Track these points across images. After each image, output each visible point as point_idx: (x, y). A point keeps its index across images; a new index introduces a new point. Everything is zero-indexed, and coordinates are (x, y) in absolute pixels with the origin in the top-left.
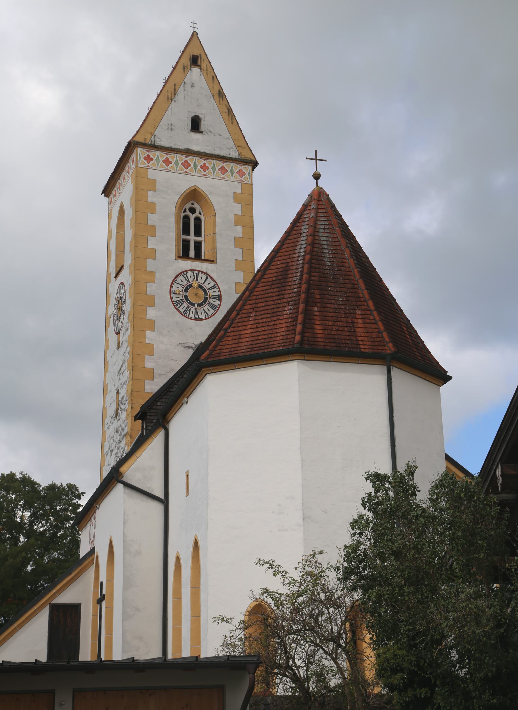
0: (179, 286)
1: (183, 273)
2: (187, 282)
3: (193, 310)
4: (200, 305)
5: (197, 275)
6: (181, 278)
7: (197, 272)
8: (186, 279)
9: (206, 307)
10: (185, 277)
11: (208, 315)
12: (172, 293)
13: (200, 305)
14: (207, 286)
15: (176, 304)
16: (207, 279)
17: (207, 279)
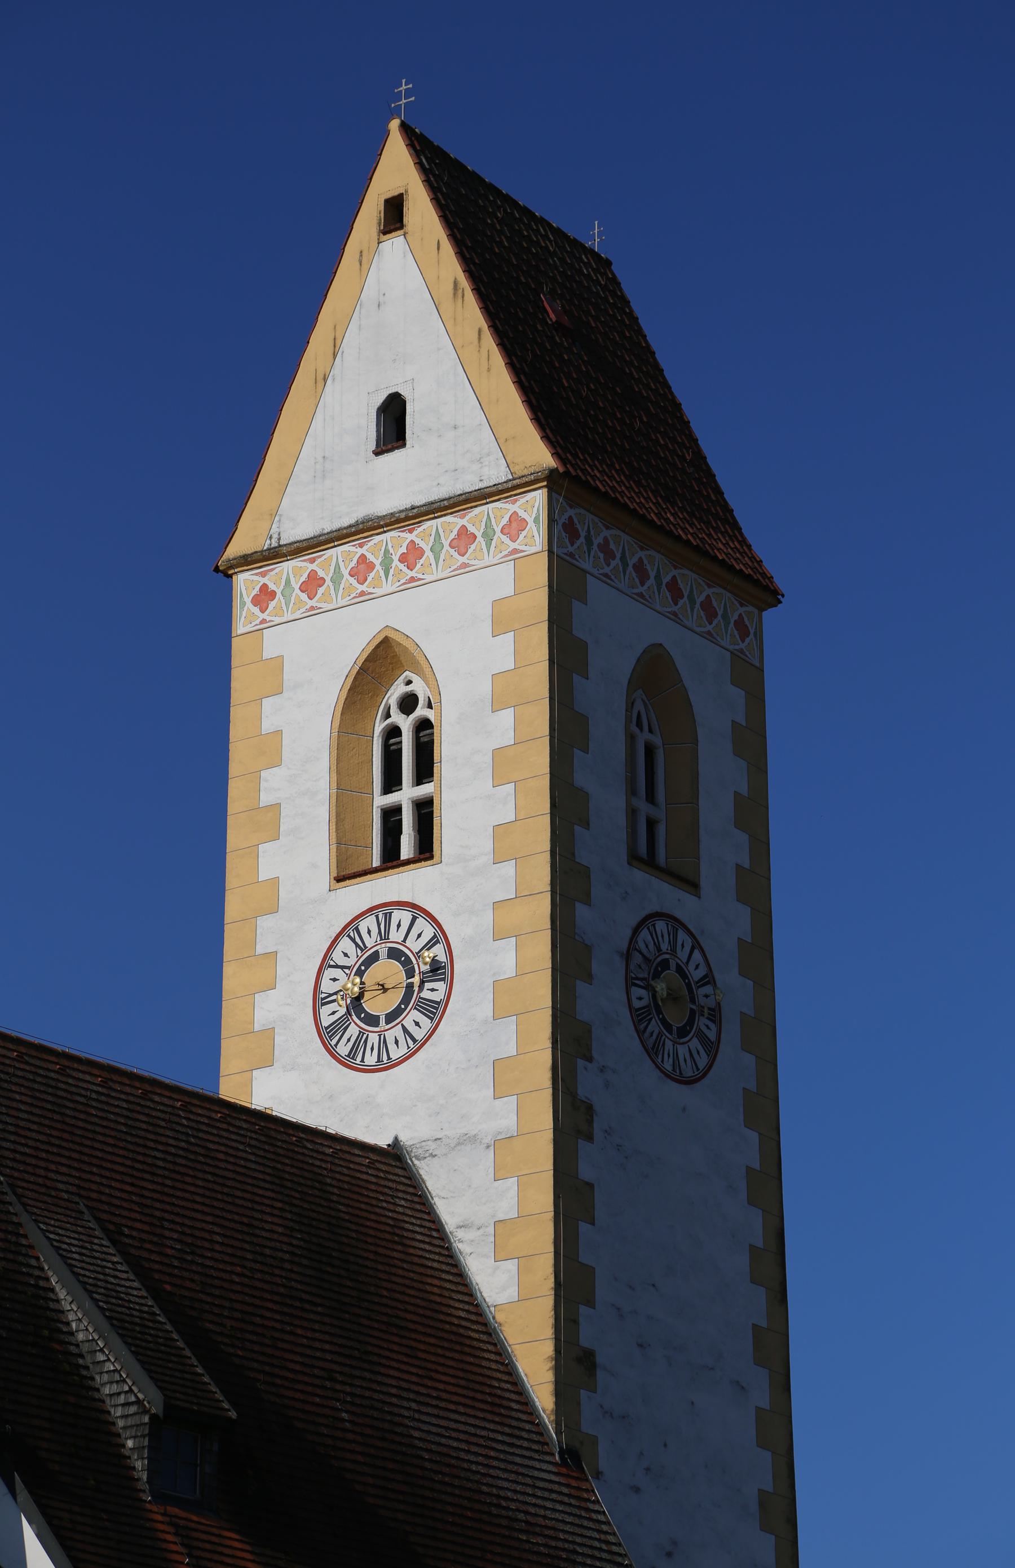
0: (337, 973)
1: (350, 929)
2: (359, 951)
3: (373, 1039)
4: (391, 1017)
5: (388, 917)
6: (346, 944)
7: (384, 910)
8: (357, 945)
9: (412, 1017)
10: (353, 940)
11: (414, 1040)
12: (319, 1000)
13: (391, 1017)
14: (414, 945)
15: (327, 1035)
16: (414, 919)
17: (414, 919)
